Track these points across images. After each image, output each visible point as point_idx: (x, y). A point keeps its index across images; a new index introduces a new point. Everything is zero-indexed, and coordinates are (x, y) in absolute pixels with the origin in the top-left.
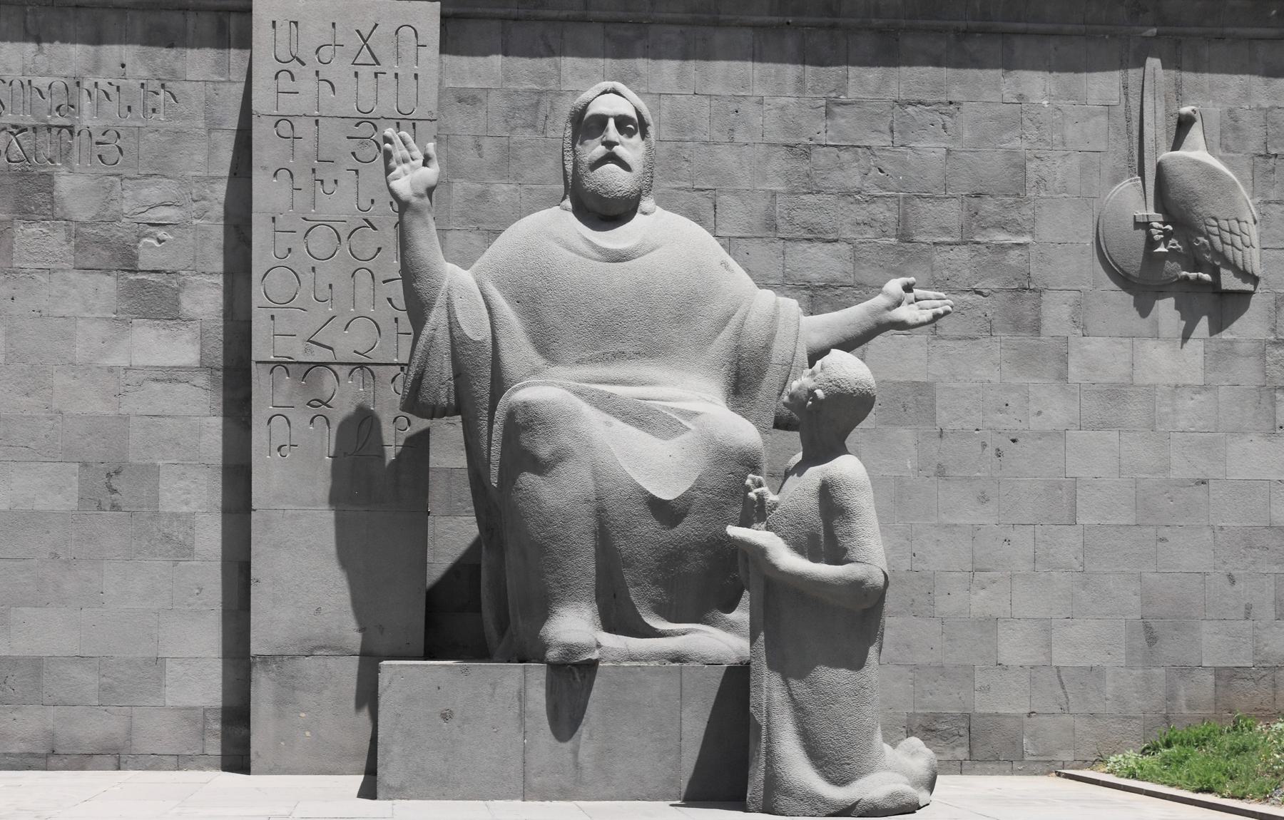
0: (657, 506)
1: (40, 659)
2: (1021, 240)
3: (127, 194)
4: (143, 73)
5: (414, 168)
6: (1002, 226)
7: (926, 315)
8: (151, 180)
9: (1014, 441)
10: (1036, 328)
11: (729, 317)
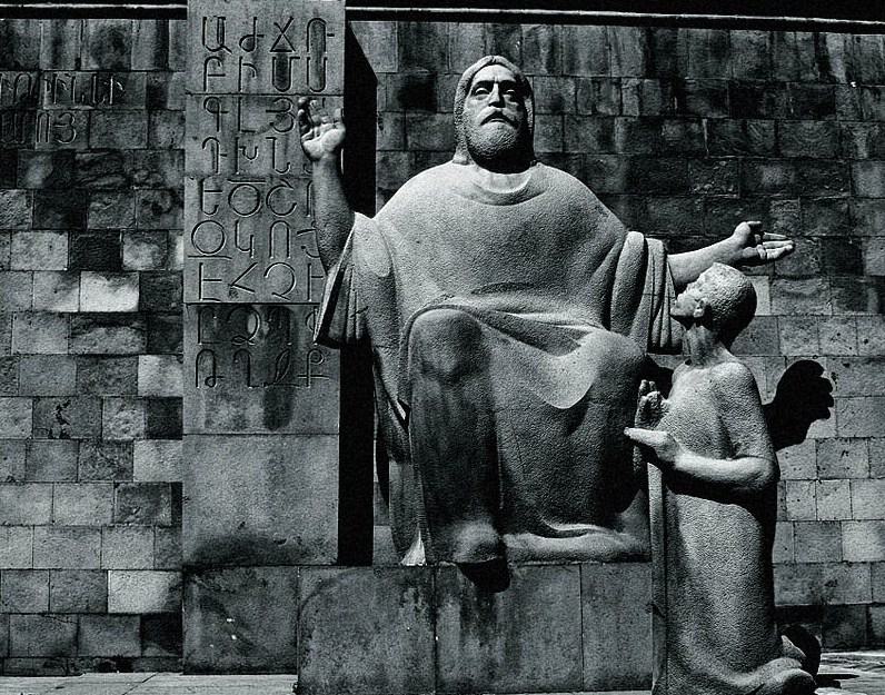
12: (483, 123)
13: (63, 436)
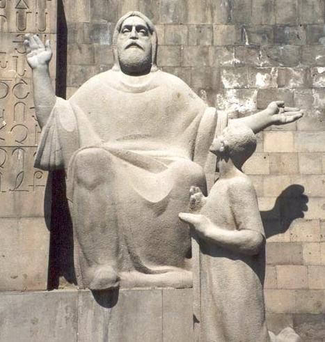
0: (150, 205)
5: (41, 51)
7: (291, 118)
11: (193, 119)
12: (128, 47)
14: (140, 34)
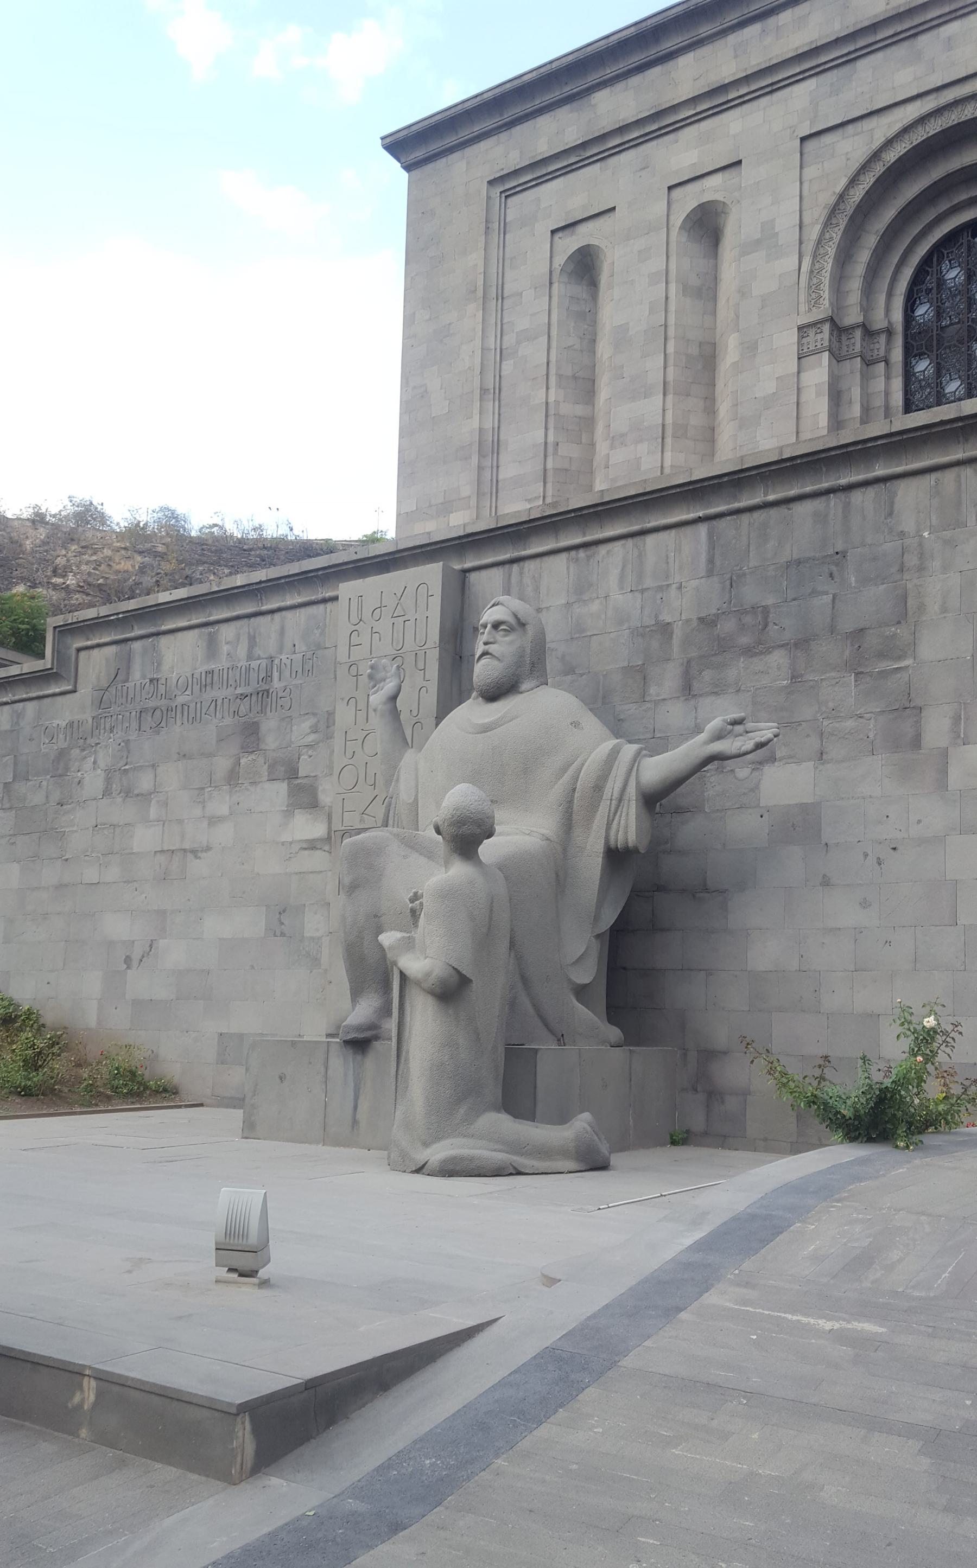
1: (242, 1034)
2: (902, 664)
3: (295, 728)
4: (304, 649)
6: (881, 655)
7: (749, 745)
8: (307, 716)
9: (894, 849)
10: (916, 743)
13: (283, 934)
14: (499, 636)
